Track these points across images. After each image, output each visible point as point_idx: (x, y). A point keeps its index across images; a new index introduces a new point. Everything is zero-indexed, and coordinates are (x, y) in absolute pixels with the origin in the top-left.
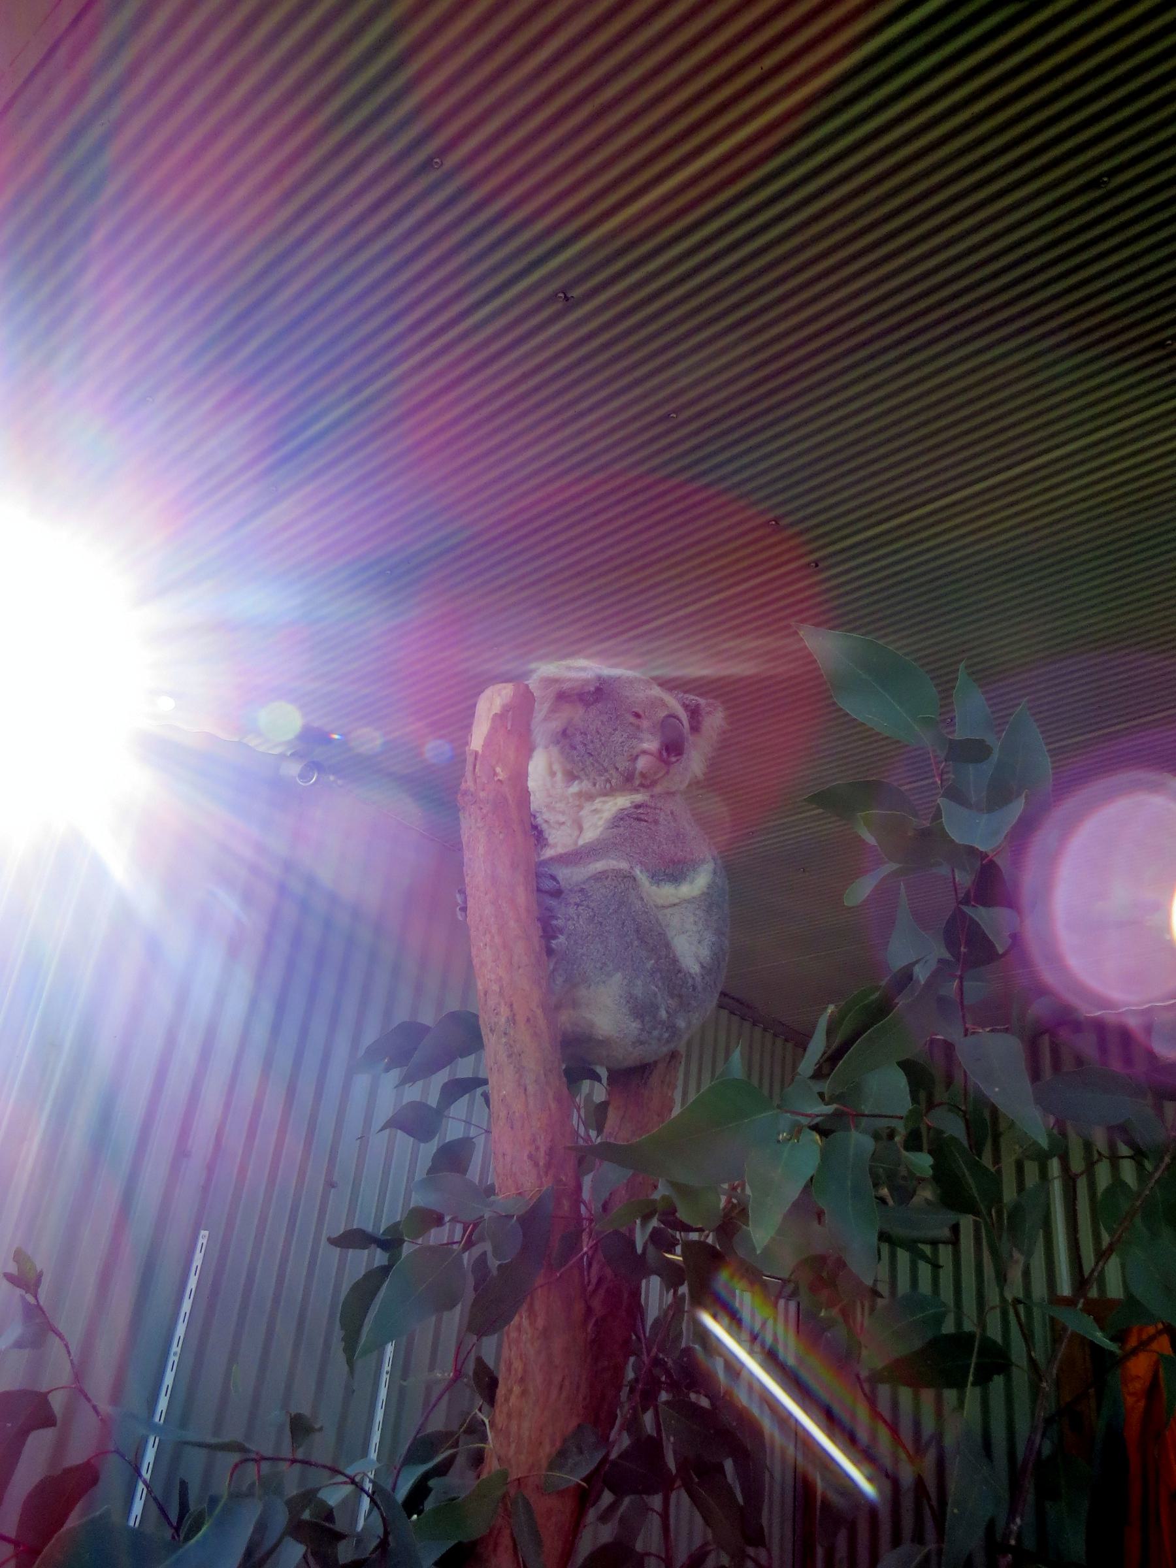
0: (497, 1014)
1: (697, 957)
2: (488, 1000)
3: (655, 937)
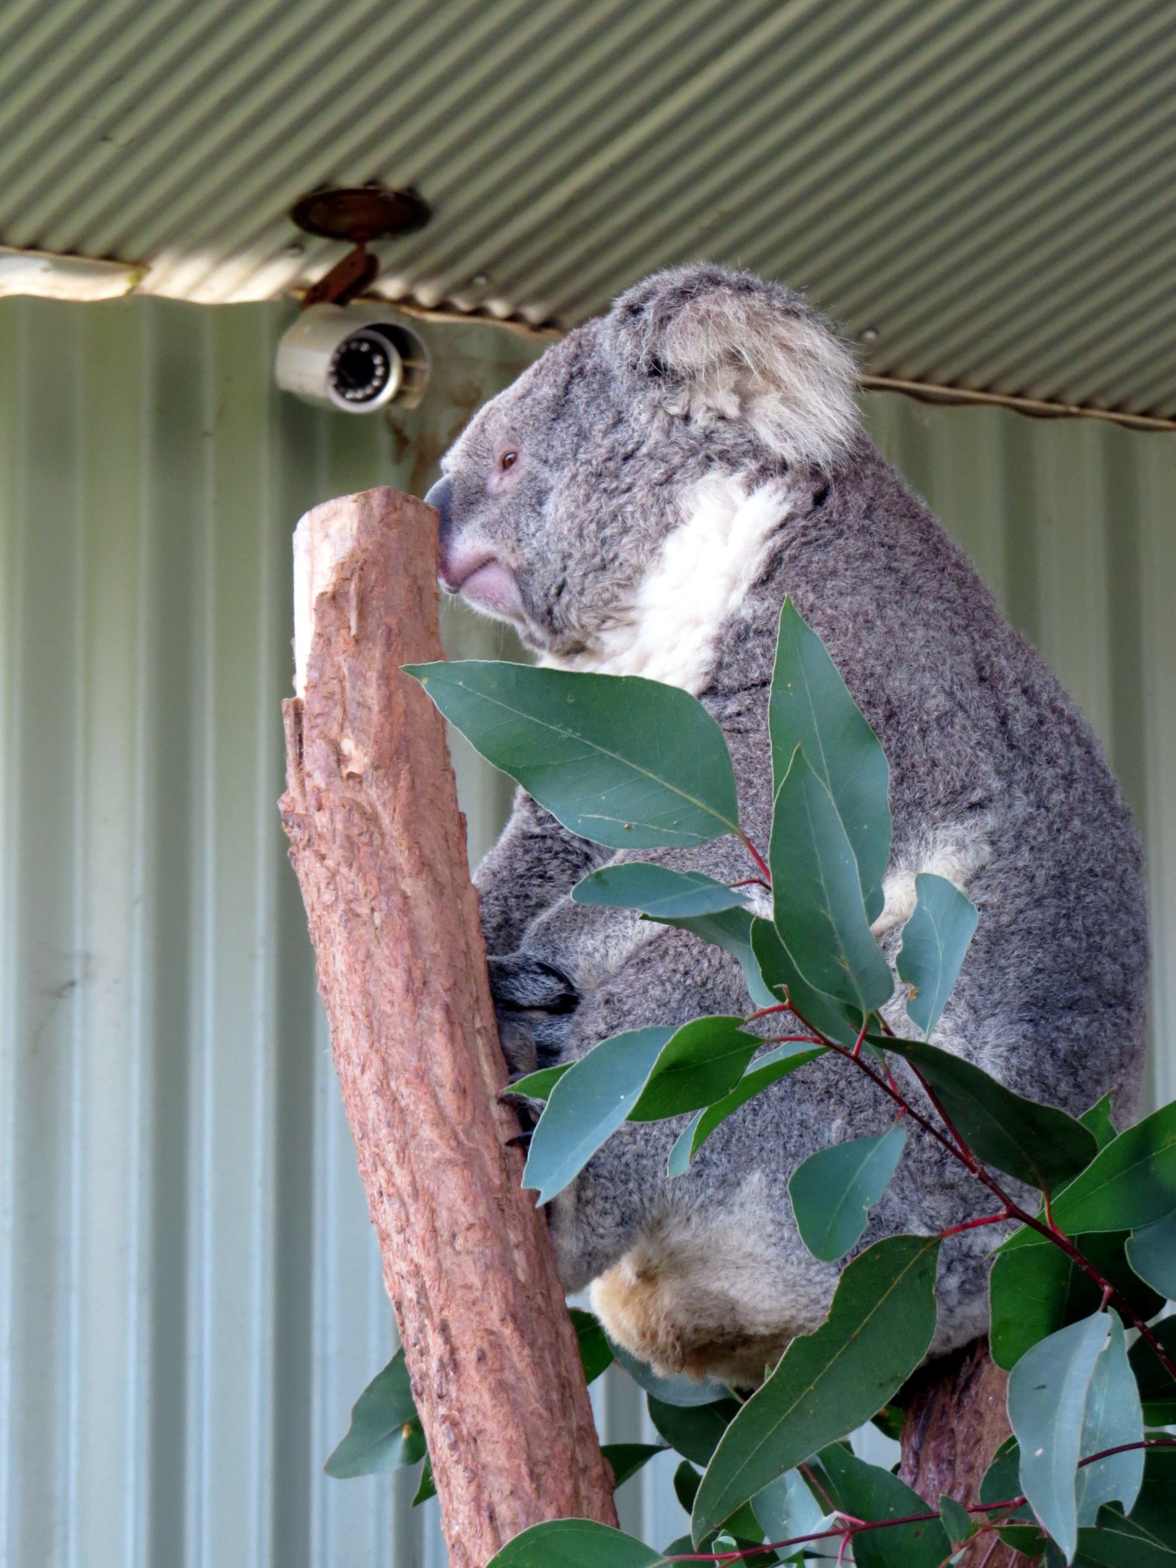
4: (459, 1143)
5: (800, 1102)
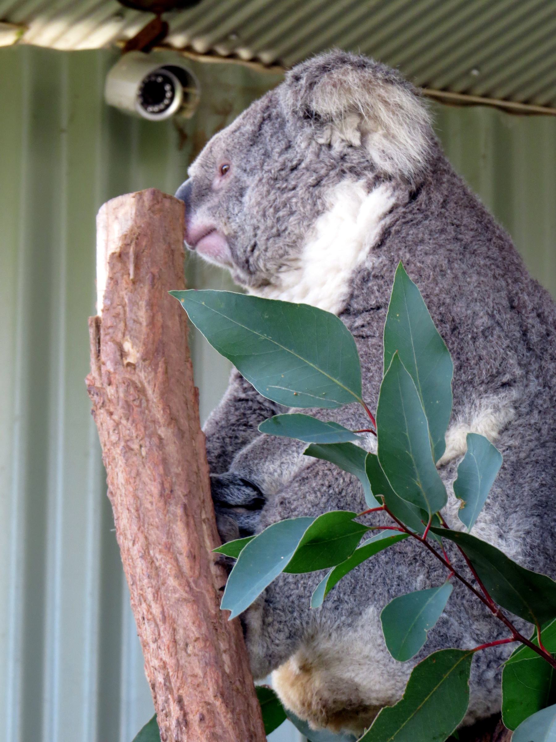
4: (191, 589)
5: (398, 565)
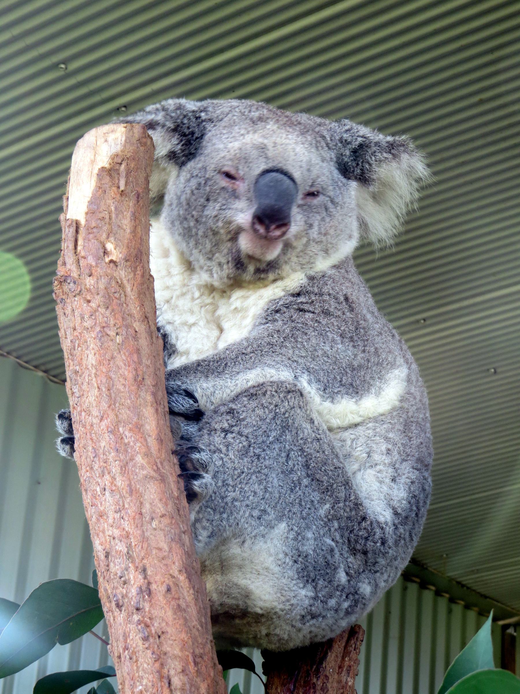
0: (125, 583)
1: (389, 501)
2: (112, 565)
3: (330, 473)
5: (314, 490)
